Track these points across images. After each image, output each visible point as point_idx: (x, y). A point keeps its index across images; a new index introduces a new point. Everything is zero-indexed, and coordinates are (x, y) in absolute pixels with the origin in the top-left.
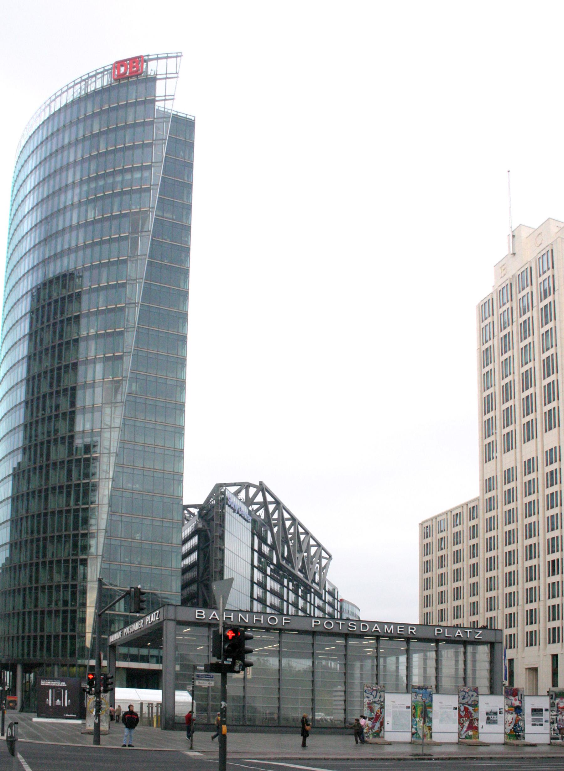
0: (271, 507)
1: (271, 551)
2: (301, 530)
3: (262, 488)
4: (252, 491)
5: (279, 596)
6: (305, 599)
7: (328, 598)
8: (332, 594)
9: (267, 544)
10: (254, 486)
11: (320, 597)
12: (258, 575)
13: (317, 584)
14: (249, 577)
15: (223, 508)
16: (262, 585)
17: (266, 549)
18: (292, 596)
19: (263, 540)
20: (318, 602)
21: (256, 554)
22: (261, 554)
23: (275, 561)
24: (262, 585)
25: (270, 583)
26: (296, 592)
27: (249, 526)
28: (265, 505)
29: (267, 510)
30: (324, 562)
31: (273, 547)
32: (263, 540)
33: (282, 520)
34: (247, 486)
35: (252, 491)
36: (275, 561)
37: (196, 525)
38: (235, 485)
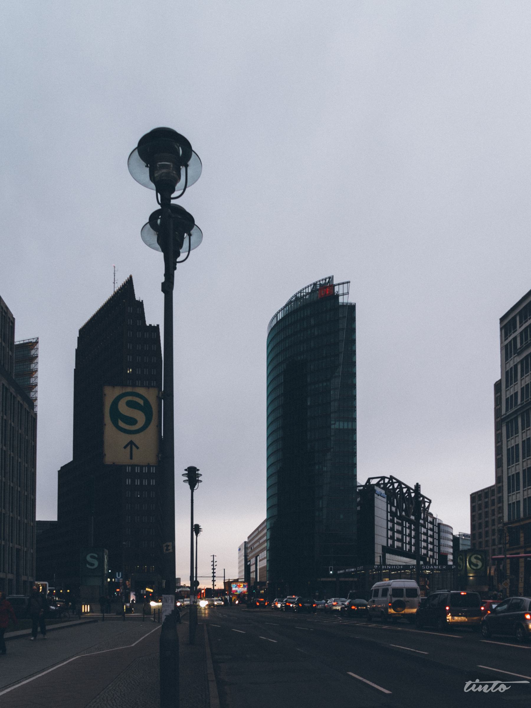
1: (396, 510)
3: (391, 478)
4: (387, 481)
7: (430, 526)
9: (394, 506)
10: (387, 478)
11: (425, 527)
12: (390, 524)
14: (386, 518)
16: (392, 529)
17: (394, 509)
19: (392, 505)
21: (389, 514)
22: (391, 512)
24: (392, 529)
25: (397, 527)
26: (410, 528)
27: (385, 500)
28: (393, 484)
30: (427, 504)
33: (401, 489)
34: (383, 478)
35: (387, 481)
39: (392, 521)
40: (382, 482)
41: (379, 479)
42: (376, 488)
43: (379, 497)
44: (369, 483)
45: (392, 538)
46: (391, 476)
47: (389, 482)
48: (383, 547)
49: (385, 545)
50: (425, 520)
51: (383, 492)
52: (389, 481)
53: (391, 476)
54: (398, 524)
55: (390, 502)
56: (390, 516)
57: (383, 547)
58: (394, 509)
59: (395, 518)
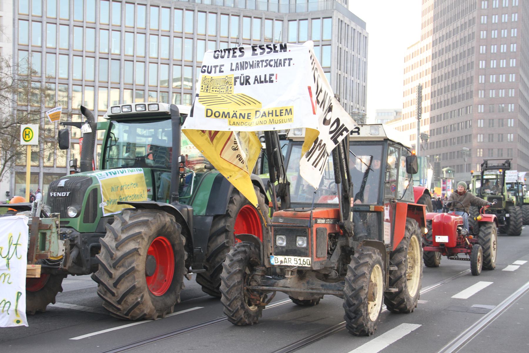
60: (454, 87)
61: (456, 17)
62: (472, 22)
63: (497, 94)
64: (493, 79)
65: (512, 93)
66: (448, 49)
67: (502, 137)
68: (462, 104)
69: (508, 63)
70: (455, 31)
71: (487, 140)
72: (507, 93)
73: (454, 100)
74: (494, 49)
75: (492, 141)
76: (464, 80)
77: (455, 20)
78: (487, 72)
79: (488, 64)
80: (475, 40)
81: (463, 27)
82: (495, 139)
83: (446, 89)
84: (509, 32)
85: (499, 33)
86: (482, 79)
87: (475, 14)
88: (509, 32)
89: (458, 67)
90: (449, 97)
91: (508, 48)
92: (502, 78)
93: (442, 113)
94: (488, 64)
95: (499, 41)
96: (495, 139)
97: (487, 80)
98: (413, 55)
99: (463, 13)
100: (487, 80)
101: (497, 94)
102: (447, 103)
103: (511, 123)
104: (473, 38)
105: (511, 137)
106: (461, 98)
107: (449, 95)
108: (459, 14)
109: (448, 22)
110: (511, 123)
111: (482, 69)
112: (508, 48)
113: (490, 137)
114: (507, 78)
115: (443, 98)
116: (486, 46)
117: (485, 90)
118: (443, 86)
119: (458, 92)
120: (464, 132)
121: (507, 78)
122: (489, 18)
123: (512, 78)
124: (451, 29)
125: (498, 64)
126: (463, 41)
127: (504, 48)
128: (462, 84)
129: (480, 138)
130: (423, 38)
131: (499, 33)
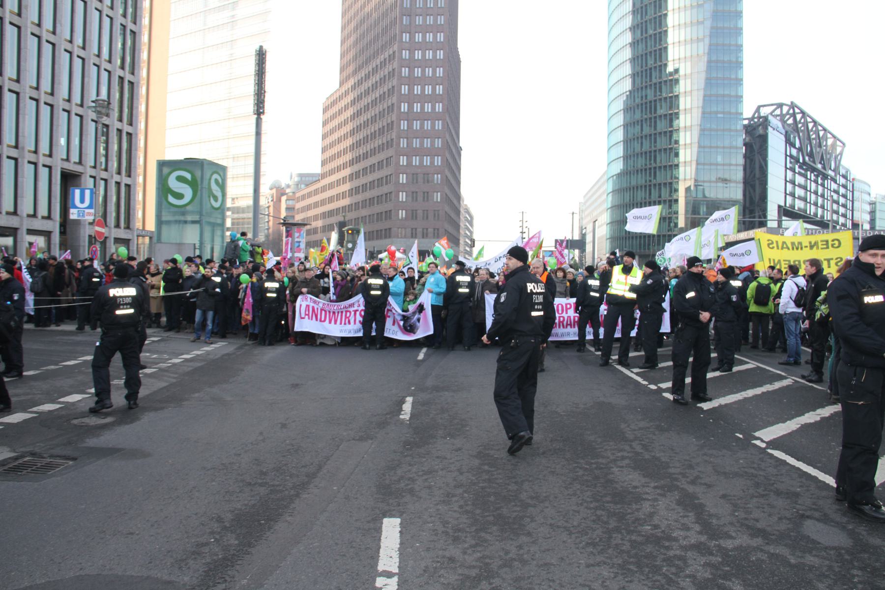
0: (799, 117)
1: (798, 153)
2: (820, 128)
3: (793, 106)
4: (785, 109)
5: (804, 188)
6: (823, 185)
7: (842, 181)
8: (845, 177)
9: (795, 147)
11: (835, 182)
12: (790, 174)
13: (834, 171)
15: (767, 129)
16: (793, 182)
17: (794, 152)
18: (813, 185)
19: (793, 145)
20: (834, 186)
22: (791, 156)
23: (801, 161)
24: (793, 182)
25: (799, 180)
26: (816, 182)
28: (794, 115)
29: (795, 119)
30: (839, 150)
31: (800, 150)
32: (793, 145)
33: (806, 124)
34: (780, 106)
36: (801, 161)
37: (744, 140)
38: (772, 105)
39: (793, 170)
40: (778, 112)
41: (775, 107)
42: (770, 118)
43: (775, 132)
44: (759, 113)
45: (793, 195)
46: (792, 103)
47: (788, 113)
48: (779, 207)
49: (783, 204)
50: (836, 170)
51: (780, 125)
52: (789, 110)
53: (792, 103)
54: (800, 174)
55: (789, 142)
56: (791, 162)
57: (779, 207)
58: (794, 152)
59: (797, 167)
60: (373, 136)
61: (375, 55)
62: (392, 57)
63: (422, 144)
64: (416, 125)
65: (438, 143)
66: (367, 92)
67: (427, 196)
68: (381, 156)
69: (433, 108)
70: (375, 71)
71: (410, 199)
72: (433, 144)
73: (373, 152)
74: (417, 90)
75: (416, 200)
76: (383, 127)
77: (374, 57)
78: (410, 117)
79: (411, 107)
80: (396, 77)
81: (383, 64)
82: (420, 199)
83: (366, 140)
84: (434, 72)
85: (423, 72)
86: (404, 125)
87: (396, 48)
88: (434, 72)
89: (377, 112)
90: (368, 149)
91: (434, 89)
92: (428, 125)
93: (361, 168)
94: (411, 107)
95: (423, 81)
96: (420, 199)
97: (410, 126)
98: (334, 103)
99: (383, 48)
100: (410, 126)
101: (422, 144)
102: (365, 156)
103: (437, 178)
104: (394, 75)
105: (438, 197)
106: (381, 148)
107: (368, 147)
108: (378, 50)
109: (367, 62)
110: (437, 178)
111: (404, 112)
112: (434, 89)
113: (413, 195)
114: (433, 125)
115: (361, 151)
116: (409, 85)
117: (407, 138)
118: (361, 137)
119: (378, 142)
120: (385, 189)
121: (433, 125)
122: (412, 53)
123: (439, 125)
124: (371, 69)
125: (422, 108)
126: (383, 80)
127: (428, 90)
128: (381, 131)
129: (402, 196)
130: (342, 84)
131: (423, 72)
